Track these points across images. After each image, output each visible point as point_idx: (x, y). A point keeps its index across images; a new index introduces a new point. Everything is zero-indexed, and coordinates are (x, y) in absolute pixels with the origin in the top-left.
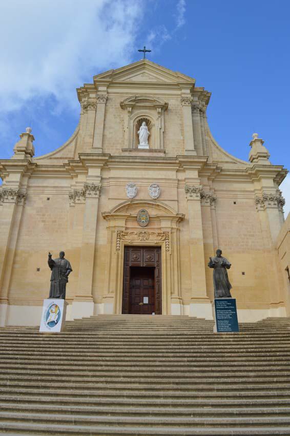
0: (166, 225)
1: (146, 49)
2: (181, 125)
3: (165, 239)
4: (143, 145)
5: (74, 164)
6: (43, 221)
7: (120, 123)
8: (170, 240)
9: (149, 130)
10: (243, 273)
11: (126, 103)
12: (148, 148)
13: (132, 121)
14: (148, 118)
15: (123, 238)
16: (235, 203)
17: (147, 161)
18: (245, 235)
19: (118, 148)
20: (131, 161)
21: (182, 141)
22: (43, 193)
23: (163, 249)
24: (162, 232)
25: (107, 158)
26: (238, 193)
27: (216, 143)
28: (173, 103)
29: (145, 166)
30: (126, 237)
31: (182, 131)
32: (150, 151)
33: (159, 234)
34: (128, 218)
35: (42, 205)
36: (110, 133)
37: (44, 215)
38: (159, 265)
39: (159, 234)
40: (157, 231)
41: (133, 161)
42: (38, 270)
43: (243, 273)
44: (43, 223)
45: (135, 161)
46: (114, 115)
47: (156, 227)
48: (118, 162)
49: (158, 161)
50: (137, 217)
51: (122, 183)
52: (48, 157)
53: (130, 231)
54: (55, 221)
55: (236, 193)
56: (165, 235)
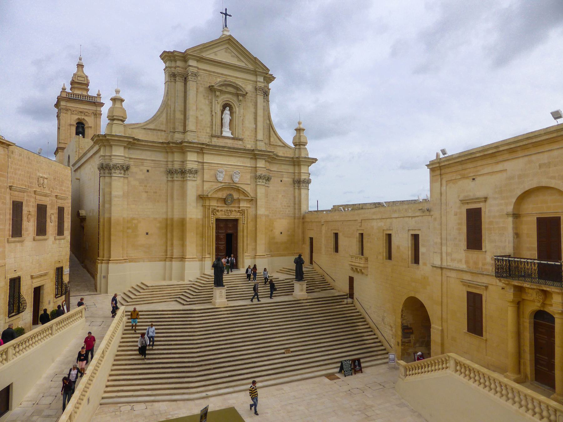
0: (243, 205)
3: (242, 215)
4: (227, 133)
5: (174, 145)
6: (147, 192)
8: (246, 215)
9: (232, 113)
11: (216, 87)
12: (230, 135)
13: (219, 106)
15: (215, 214)
16: (281, 181)
17: (232, 150)
18: (285, 206)
20: (221, 149)
21: (255, 130)
22: (143, 165)
24: (240, 210)
25: (204, 146)
26: (285, 174)
28: (249, 88)
29: (230, 153)
30: (217, 213)
32: (233, 139)
33: (239, 211)
34: (218, 199)
36: (201, 115)
37: (146, 186)
38: (237, 233)
40: (237, 209)
41: (222, 149)
42: (147, 234)
43: (281, 233)
44: (146, 194)
45: (224, 149)
46: (204, 96)
47: (237, 205)
49: (240, 151)
51: (213, 167)
52: (141, 127)
54: (156, 192)
55: (283, 173)
56: (242, 212)
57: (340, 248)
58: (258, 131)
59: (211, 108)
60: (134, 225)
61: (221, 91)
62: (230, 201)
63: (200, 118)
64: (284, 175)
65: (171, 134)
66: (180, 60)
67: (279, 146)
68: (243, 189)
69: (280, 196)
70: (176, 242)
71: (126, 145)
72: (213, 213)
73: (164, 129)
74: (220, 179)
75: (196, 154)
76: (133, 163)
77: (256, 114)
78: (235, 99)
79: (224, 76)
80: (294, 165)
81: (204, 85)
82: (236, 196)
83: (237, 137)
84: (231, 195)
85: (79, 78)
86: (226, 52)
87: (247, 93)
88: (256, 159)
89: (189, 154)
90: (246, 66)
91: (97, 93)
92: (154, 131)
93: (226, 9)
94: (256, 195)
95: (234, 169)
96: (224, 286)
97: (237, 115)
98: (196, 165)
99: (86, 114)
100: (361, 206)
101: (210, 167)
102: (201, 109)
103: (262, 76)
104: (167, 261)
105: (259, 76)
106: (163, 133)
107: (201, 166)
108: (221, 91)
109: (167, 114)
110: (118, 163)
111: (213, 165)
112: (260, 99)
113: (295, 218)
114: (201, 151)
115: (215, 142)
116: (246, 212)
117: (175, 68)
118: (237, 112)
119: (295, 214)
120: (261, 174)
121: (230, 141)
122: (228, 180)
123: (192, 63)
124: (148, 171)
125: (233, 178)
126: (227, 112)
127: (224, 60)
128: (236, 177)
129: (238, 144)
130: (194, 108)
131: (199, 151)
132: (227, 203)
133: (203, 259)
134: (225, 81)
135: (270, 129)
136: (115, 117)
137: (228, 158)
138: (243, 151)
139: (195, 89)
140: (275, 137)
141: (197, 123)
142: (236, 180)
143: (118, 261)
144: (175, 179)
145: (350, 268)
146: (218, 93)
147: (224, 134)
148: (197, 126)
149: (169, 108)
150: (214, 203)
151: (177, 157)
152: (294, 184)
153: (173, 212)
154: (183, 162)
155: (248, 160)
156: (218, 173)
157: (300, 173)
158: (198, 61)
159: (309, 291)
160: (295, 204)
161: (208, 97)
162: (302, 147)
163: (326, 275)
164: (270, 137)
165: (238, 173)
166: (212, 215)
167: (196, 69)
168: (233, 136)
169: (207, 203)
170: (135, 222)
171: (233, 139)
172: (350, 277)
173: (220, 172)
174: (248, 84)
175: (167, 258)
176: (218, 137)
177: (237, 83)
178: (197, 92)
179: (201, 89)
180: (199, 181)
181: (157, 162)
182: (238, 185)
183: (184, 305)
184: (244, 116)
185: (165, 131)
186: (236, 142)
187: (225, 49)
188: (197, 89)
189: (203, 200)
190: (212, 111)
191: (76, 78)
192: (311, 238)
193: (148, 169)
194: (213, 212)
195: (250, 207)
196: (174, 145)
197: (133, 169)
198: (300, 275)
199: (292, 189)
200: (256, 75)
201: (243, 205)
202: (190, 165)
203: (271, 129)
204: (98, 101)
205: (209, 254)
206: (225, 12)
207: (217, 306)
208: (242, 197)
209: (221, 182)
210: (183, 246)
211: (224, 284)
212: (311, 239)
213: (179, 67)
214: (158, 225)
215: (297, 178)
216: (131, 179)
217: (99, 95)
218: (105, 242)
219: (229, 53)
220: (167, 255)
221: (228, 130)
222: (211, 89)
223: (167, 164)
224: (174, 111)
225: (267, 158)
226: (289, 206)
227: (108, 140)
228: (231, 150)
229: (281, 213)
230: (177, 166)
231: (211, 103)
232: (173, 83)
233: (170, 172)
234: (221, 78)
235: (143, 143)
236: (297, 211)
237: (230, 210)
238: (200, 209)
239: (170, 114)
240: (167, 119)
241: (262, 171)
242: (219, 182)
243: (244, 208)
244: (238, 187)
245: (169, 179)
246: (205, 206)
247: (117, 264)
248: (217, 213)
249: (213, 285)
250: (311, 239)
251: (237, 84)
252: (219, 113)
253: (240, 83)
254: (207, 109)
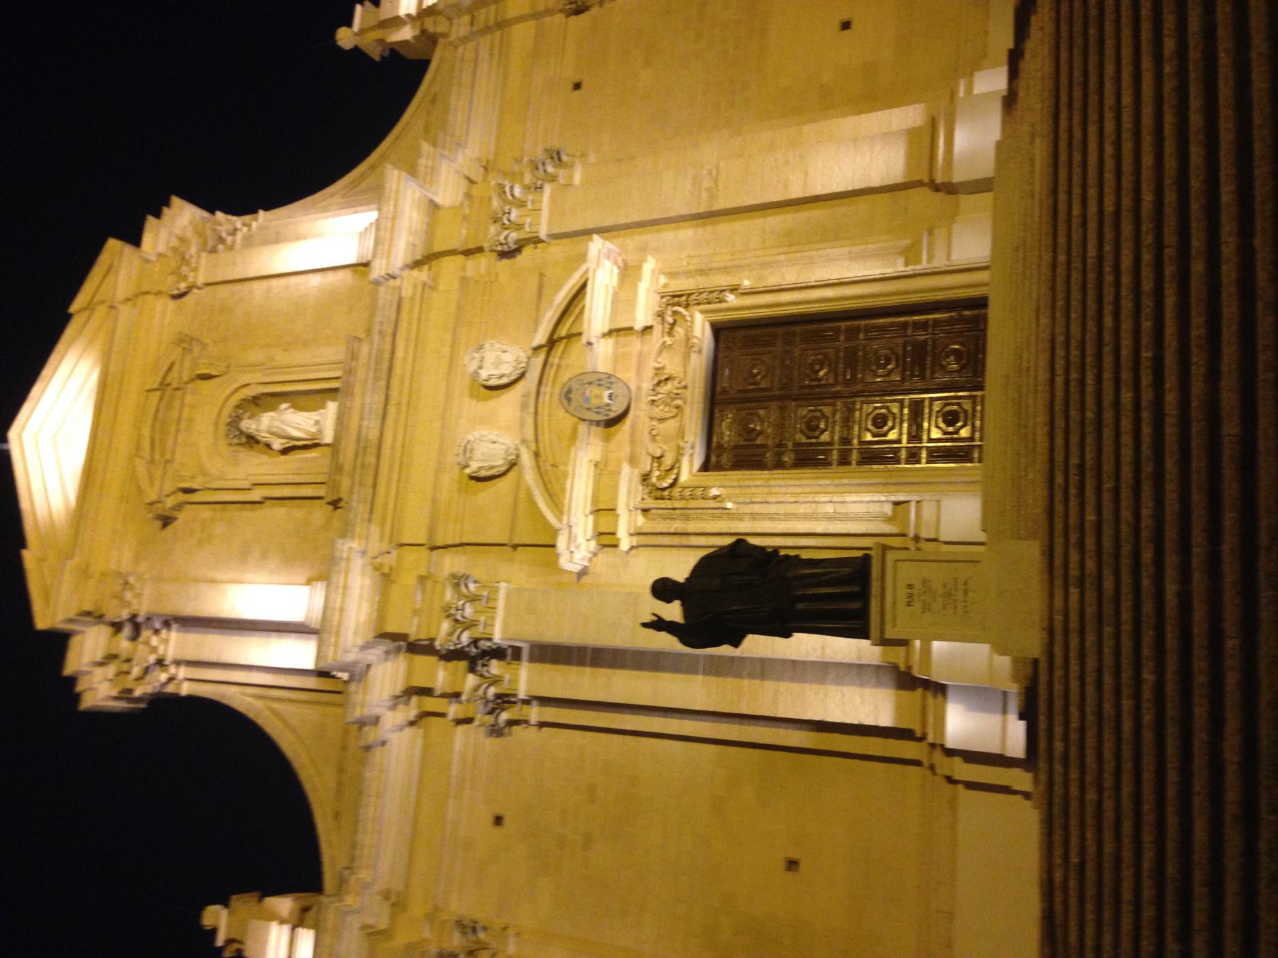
6: (588, 840)
10: (846, 25)
30: (668, 461)
42: (792, 865)
43: (846, 25)
46: (200, 543)
62: (607, 393)
72: (664, 489)
84: (567, 395)
124: (498, 820)
166: (676, 492)
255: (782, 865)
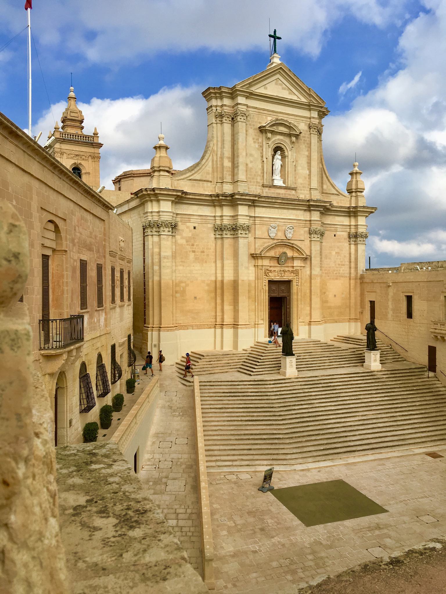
0: (297, 263)
1: (278, 35)
2: (307, 156)
5: (223, 198)
6: (194, 252)
7: (258, 149)
8: (300, 276)
10: (335, 296)
13: (270, 149)
14: (282, 146)
16: (335, 235)
18: (339, 265)
19: (258, 180)
20: (274, 201)
23: (294, 284)
25: (257, 199)
26: (339, 227)
27: (327, 173)
28: (302, 127)
29: (283, 205)
30: (270, 274)
31: (309, 164)
32: (286, 188)
33: (292, 272)
34: (271, 258)
35: (190, 235)
36: (251, 162)
37: (193, 245)
39: (292, 272)
40: (291, 269)
43: (335, 296)
44: (193, 254)
46: (254, 139)
47: (290, 265)
48: (263, 201)
49: (293, 203)
50: (279, 257)
52: (187, 178)
53: (272, 269)
54: (203, 252)
56: (296, 272)
57: (415, 313)
58: (312, 178)
59: (262, 153)
60: (182, 289)
61: (272, 132)
63: (250, 165)
64: (338, 229)
65: (219, 185)
66: (227, 97)
67: (333, 194)
68: (298, 246)
69: (334, 253)
70: (228, 308)
71: (174, 199)
73: (210, 180)
74: (272, 235)
75: (247, 207)
76: (179, 219)
77: (309, 157)
78: (287, 140)
79: (274, 114)
80: (350, 216)
81: (254, 125)
82: (290, 253)
83: (289, 186)
85: (73, 114)
86: (276, 84)
87: (300, 133)
88: (310, 211)
89: (240, 207)
90: (300, 100)
91: (93, 131)
92: (200, 182)
93: (275, 30)
94: (311, 253)
95: (289, 224)
96: (294, 355)
97: (289, 160)
98: (248, 220)
99: (83, 157)
100: (440, 264)
101: (261, 222)
102: (251, 155)
103: (316, 111)
104: (217, 328)
105: (313, 110)
106: (209, 184)
107: (252, 221)
108: (272, 132)
109: (213, 161)
110: (167, 220)
111: (265, 219)
112: (314, 139)
113: (350, 279)
114: (253, 204)
115: (266, 192)
116: (300, 272)
117: (222, 106)
118: (289, 157)
119: (350, 273)
120: (316, 228)
121: (282, 191)
122: (281, 236)
123: (241, 100)
125: (286, 234)
126: (278, 156)
127: (275, 94)
128: (290, 233)
129: (291, 195)
130: (244, 154)
131: (250, 203)
132: (280, 263)
133: (256, 325)
134: (277, 120)
135: (322, 175)
136: (161, 168)
137: (280, 211)
138: (297, 203)
139: (245, 131)
140: (329, 184)
141: (246, 171)
142: (289, 236)
143: (169, 329)
144: (225, 236)
145: (433, 336)
146: (269, 135)
147: (276, 183)
148: (247, 175)
149: (215, 155)
150: (266, 262)
151: (227, 211)
152: (350, 238)
153: (223, 273)
154: (235, 217)
155: (302, 212)
156: (271, 228)
157: (356, 226)
158: (247, 97)
159: (382, 362)
160: (350, 262)
161: (258, 139)
162: (359, 194)
163: (394, 344)
164: (322, 183)
165: (291, 228)
167: (245, 107)
168: (285, 185)
169: (260, 262)
170: (183, 285)
171: (286, 188)
172: (429, 347)
173: (272, 228)
174: (302, 121)
175: (216, 325)
176: (270, 187)
177: (290, 121)
178: (246, 135)
179: (251, 131)
180: (251, 239)
181: (204, 218)
182: (292, 242)
183: (250, 375)
184: (297, 161)
185: (211, 182)
186: (289, 192)
187: (275, 81)
188: (246, 131)
189: (255, 259)
190: (262, 157)
191: (69, 113)
192: (371, 302)
193: (195, 226)
194: (265, 273)
195: (304, 267)
196: (223, 198)
197: (181, 226)
198: (372, 345)
199: (346, 244)
200: (310, 110)
201: (297, 263)
202: (242, 221)
203: (324, 175)
204: (95, 141)
205: (263, 320)
206: (273, 34)
207: (287, 377)
208: (296, 255)
209: (273, 239)
210: (236, 311)
211: (294, 352)
212: (372, 303)
213: (225, 105)
214: (206, 288)
215: (353, 231)
216: (178, 237)
217: (96, 134)
218: (155, 308)
219: (280, 85)
220: (216, 322)
221: (280, 178)
222: (262, 130)
223: (215, 220)
224: (222, 158)
225: (322, 209)
226: (344, 265)
227: (156, 195)
228: (284, 202)
229: (335, 272)
230: (226, 222)
231: (262, 147)
232: (219, 125)
233: (219, 229)
234: (271, 116)
235: (191, 197)
236: (353, 271)
237: (283, 271)
238: (252, 269)
239: (217, 161)
240: (213, 168)
241: (317, 225)
242: (272, 239)
243: (298, 268)
244: (293, 244)
245: (218, 236)
246: (257, 266)
247: (168, 331)
248: (270, 274)
249: (281, 353)
250: (372, 303)
251: (290, 123)
252: (270, 158)
253: (292, 120)
254: (257, 154)
255: (195, 296)
